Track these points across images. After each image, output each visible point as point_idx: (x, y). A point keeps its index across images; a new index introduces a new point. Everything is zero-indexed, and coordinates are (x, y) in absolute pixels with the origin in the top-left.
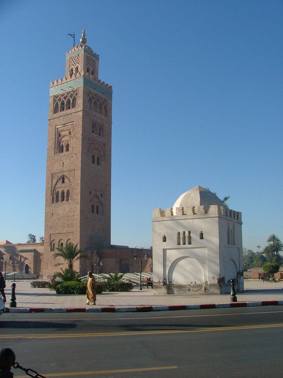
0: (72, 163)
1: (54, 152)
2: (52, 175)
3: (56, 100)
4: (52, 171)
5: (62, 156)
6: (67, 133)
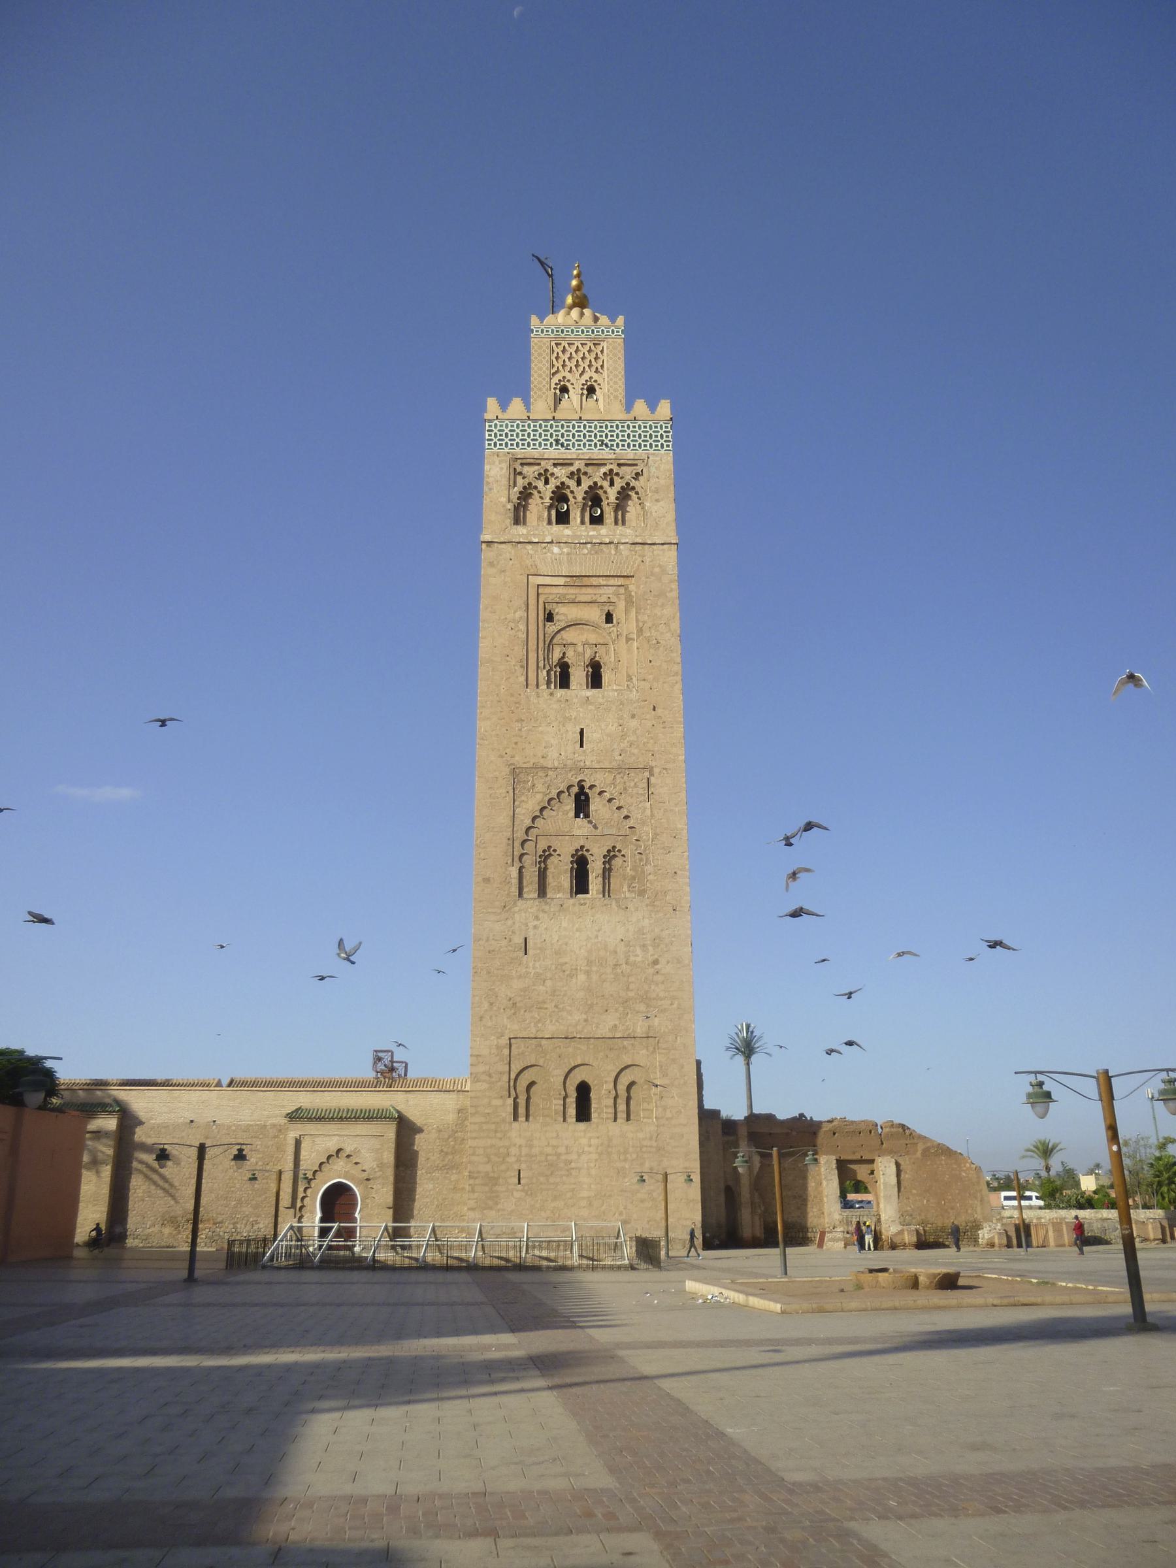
0: (633, 738)
1: (522, 679)
3: (517, 473)
4: (517, 758)
6: (595, 615)
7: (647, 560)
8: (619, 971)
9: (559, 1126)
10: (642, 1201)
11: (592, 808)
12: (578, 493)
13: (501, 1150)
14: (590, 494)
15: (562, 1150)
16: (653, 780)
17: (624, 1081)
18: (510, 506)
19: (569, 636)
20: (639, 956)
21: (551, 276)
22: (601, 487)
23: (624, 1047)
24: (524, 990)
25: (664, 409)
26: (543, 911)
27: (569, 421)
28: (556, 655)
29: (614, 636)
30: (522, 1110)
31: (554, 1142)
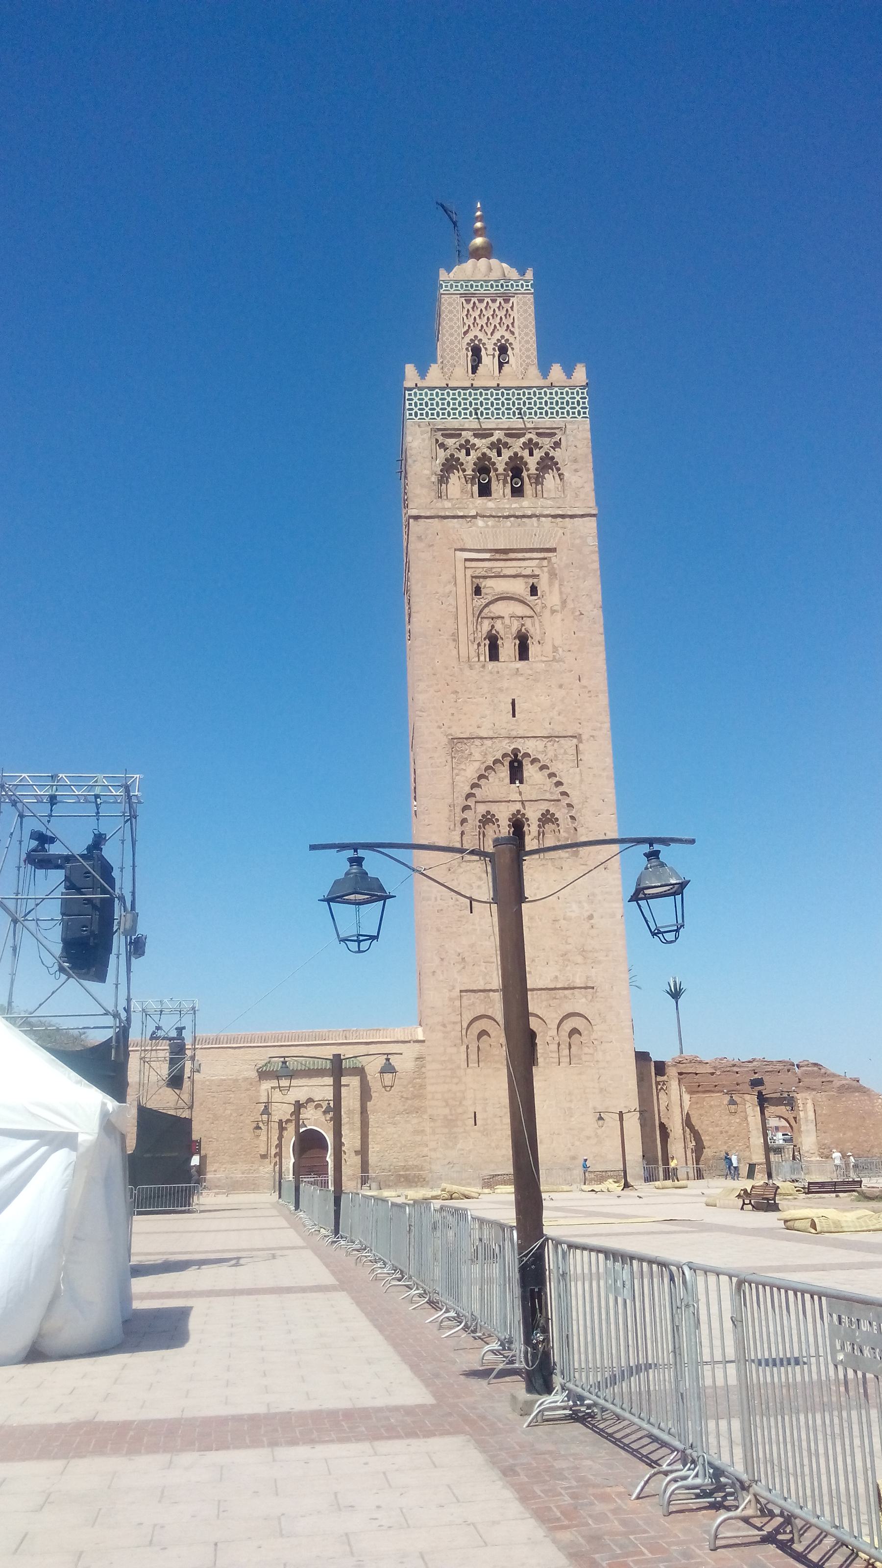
5: (507, 672)
6: (520, 587)
8: (557, 926)
10: (588, 1138)
12: (501, 463)
14: (511, 465)
16: (581, 746)
18: (434, 479)
19: (499, 608)
22: (522, 458)
23: (565, 997)
24: (472, 946)
25: (580, 374)
27: (487, 388)
28: (486, 626)
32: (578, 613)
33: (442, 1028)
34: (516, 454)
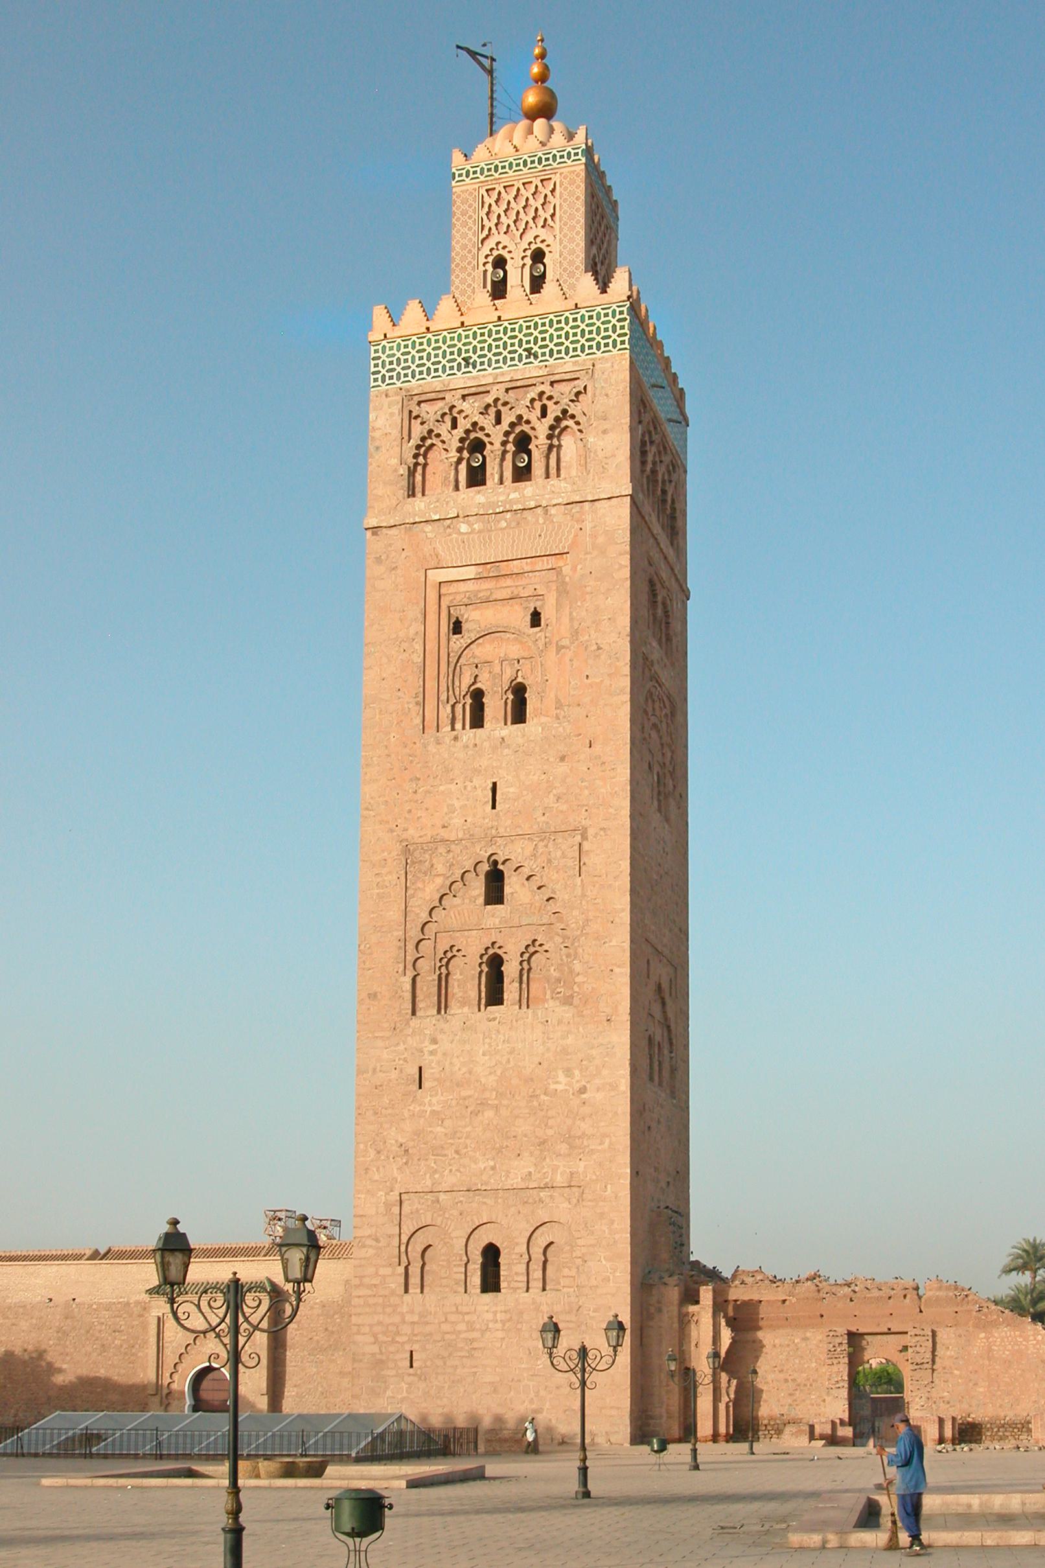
1: (419, 720)
2: (406, 851)
4: (411, 831)
7: (588, 526)
9: (460, 1298)
11: (507, 890)
12: (495, 436)
13: (390, 1328)
15: (462, 1327)
16: (586, 846)
17: (540, 1241)
18: (403, 470)
19: (483, 650)
20: (561, 1082)
21: (490, 72)
23: (541, 1201)
26: (442, 1031)
27: (482, 326)
28: (467, 680)
29: (541, 644)
30: (415, 1280)
31: (452, 1318)
32: (595, 647)
33: (374, 1243)
34: (520, 417)
